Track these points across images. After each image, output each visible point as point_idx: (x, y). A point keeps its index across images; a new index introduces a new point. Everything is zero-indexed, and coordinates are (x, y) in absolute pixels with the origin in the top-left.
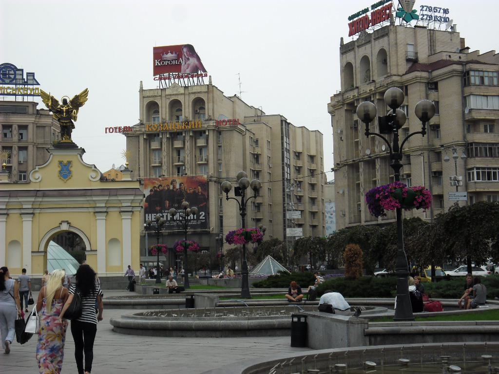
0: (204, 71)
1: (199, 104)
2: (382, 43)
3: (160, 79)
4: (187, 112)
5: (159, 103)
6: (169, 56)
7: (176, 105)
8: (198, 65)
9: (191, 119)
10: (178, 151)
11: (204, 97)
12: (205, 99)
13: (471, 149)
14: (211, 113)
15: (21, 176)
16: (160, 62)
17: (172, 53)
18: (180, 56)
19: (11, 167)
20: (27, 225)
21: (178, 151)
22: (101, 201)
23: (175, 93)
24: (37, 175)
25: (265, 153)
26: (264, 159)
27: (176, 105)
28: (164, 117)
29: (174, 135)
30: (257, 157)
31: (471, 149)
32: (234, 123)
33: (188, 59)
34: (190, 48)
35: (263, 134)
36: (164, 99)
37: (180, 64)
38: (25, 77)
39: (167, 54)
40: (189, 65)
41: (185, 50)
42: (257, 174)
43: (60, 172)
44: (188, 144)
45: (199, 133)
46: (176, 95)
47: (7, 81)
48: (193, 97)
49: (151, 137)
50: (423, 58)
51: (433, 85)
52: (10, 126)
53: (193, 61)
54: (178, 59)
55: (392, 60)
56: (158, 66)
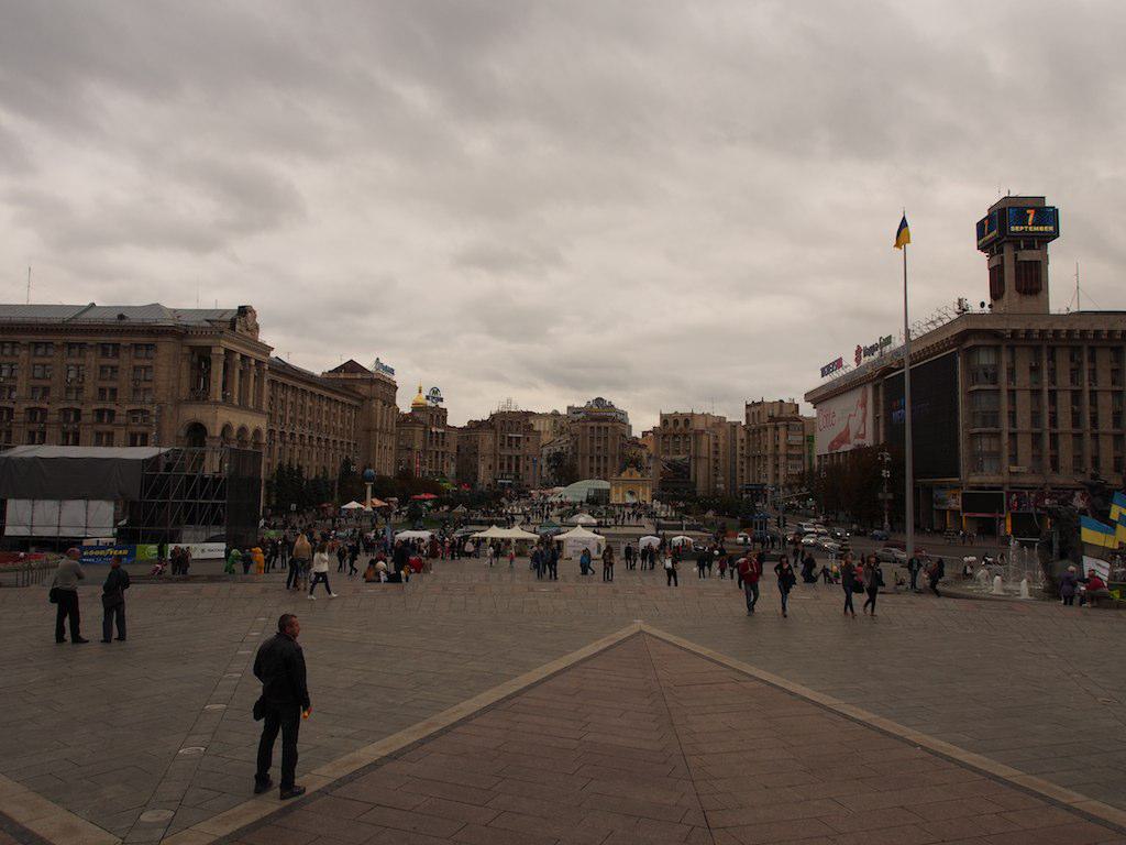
1: (687, 422)
2: (758, 408)
4: (681, 424)
7: (676, 422)
13: (788, 457)
25: (722, 441)
26: (720, 446)
27: (676, 422)
29: (675, 436)
30: (716, 445)
31: (788, 457)
32: (703, 431)
35: (721, 433)
42: (716, 453)
45: (686, 435)
49: (665, 436)
50: (776, 415)
51: (777, 428)
55: (762, 417)
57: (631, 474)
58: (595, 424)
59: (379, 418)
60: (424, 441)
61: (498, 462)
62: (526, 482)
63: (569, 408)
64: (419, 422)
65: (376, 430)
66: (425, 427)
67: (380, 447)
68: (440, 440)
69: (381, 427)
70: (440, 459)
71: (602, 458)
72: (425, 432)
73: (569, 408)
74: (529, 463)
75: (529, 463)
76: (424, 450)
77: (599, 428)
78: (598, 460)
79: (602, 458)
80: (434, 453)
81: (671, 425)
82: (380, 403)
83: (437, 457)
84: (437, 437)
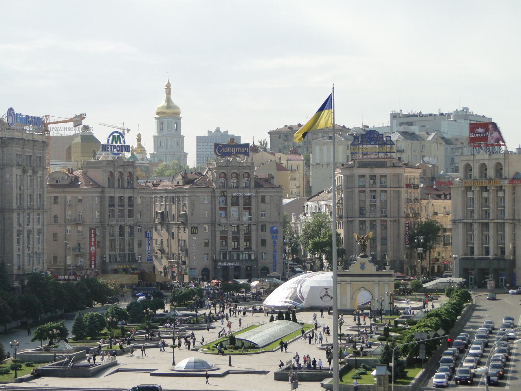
0: (503, 141)
3: (474, 146)
5: (472, 165)
6: (480, 130)
8: (499, 138)
9: (493, 178)
10: (487, 199)
11: (502, 162)
12: (503, 164)
14: (507, 174)
15: (382, 211)
16: (473, 134)
17: (482, 128)
18: (487, 130)
19: (375, 205)
20: (348, 287)
21: (487, 199)
22: (376, 279)
23: (482, 158)
24: (352, 269)
27: (483, 167)
28: (475, 175)
33: (493, 133)
34: (494, 125)
36: (475, 162)
37: (487, 137)
38: (385, 139)
39: (478, 129)
40: (493, 137)
41: (490, 126)
43: (361, 267)
44: (491, 195)
46: (483, 160)
47: (372, 143)
48: (495, 162)
52: (375, 176)
53: (496, 134)
54: (486, 133)
56: (472, 137)
57: (363, 267)
58: (365, 171)
59: (15, 192)
60: (102, 213)
61: (218, 234)
62: (262, 263)
63: (394, 116)
64: (96, 184)
65: (12, 211)
66: (102, 192)
67: (19, 233)
68: (126, 209)
69: (19, 208)
70: (127, 234)
71: (378, 224)
72: (102, 198)
73: (394, 116)
74: (267, 235)
75: (267, 235)
76: (102, 225)
77: (373, 177)
78: (373, 227)
79: (378, 224)
80: (117, 229)
81: (476, 173)
82: (16, 171)
83: (122, 234)
84: (122, 206)
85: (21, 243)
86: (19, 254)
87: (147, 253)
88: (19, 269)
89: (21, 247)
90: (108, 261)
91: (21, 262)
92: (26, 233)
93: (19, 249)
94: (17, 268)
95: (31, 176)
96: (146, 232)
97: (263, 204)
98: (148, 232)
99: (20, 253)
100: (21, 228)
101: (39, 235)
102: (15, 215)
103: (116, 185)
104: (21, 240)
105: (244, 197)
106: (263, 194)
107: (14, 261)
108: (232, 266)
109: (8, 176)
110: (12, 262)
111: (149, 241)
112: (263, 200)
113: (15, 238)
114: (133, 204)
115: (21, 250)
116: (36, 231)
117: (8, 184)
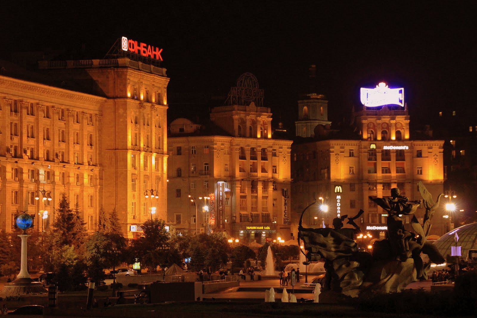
85: (137, 190)
86: (133, 201)
87: (283, 214)
88: (134, 218)
89: (136, 193)
90: (238, 220)
91: (137, 211)
92: (142, 178)
93: (134, 195)
94: (133, 217)
95: (148, 114)
96: (283, 190)
97: (419, 159)
98: (285, 189)
99: (136, 200)
100: (136, 172)
101: (158, 183)
102: (129, 156)
103: (248, 135)
104: (137, 186)
105: (397, 151)
106: (418, 148)
107: (128, 209)
108: (382, 231)
109: (121, 111)
110: (126, 210)
111: (285, 200)
112: (419, 154)
113: (129, 183)
114: (267, 157)
115: (136, 196)
116: (154, 177)
117: (121, 120)
